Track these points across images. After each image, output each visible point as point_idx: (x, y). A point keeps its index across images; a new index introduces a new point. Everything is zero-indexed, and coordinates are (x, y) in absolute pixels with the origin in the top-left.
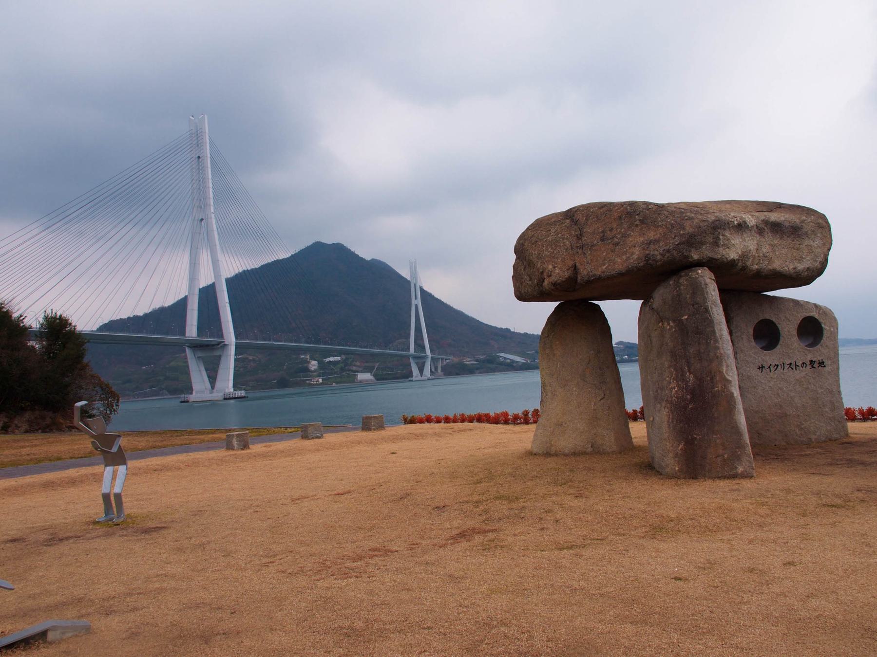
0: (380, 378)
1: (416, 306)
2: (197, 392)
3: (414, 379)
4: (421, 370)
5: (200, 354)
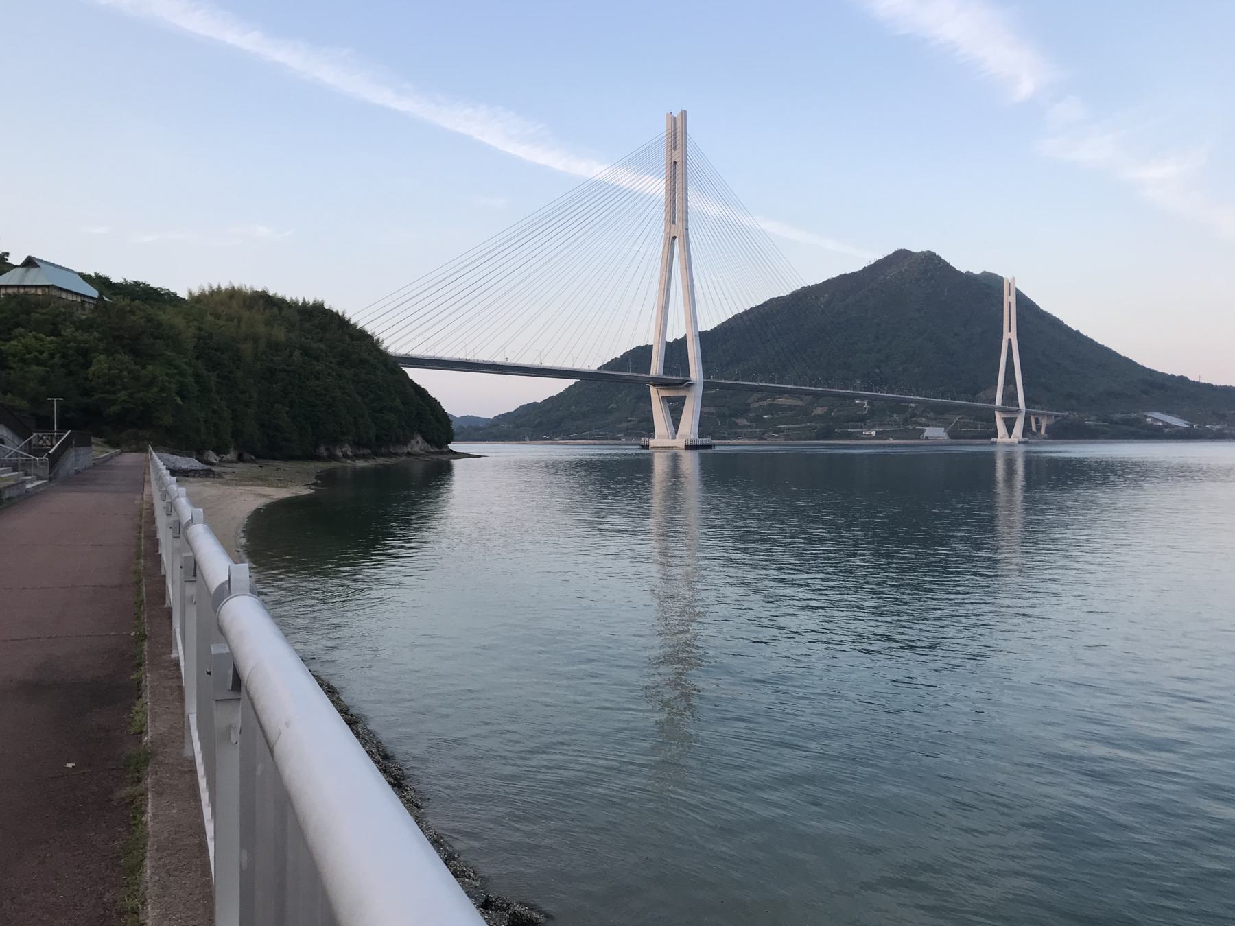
1: (1010, 341)
2: (659, 436)
3: (999, 440)
4: (1010, 430)
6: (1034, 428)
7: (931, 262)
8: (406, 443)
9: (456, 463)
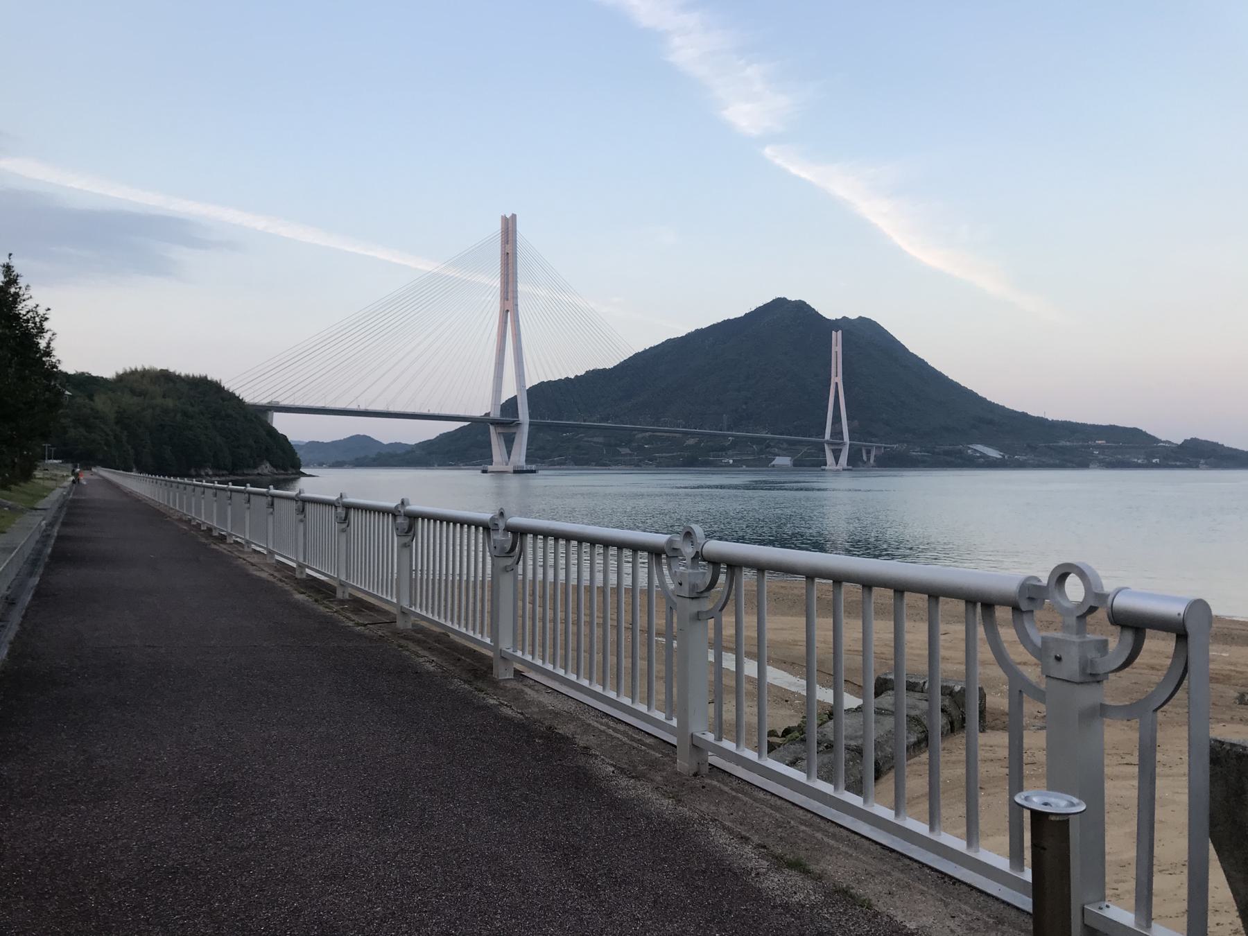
0: (798, 464)
4: (837, 459)
5: (500, 430)
6: (865, 458)
7: (801, 309)
8: (256, 467)
9: (303, 479)
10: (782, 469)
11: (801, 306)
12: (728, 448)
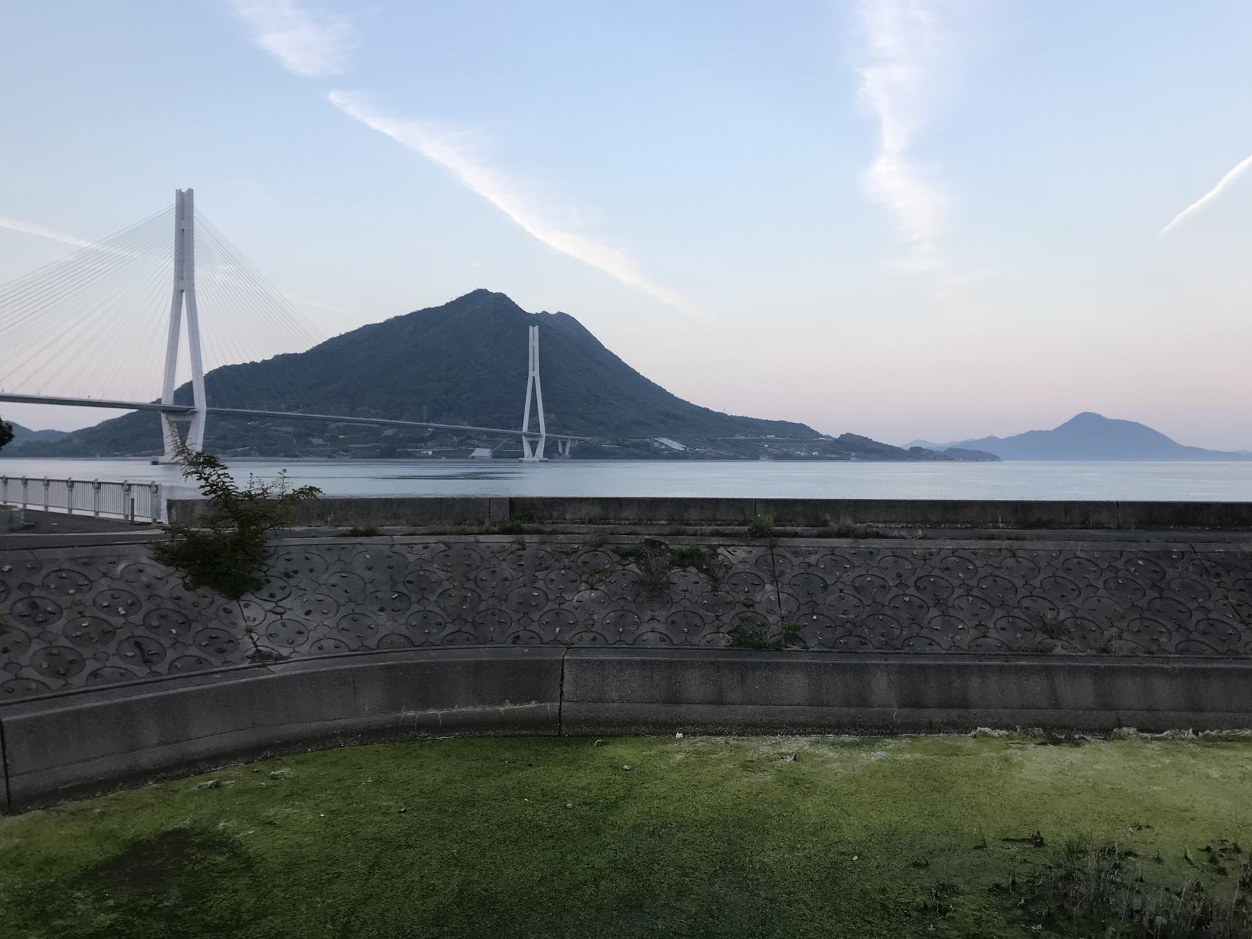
0: (497, 456)
5: (173, 418)
10: (481, 460)
11: (501, 298)
12: (429, 439)
